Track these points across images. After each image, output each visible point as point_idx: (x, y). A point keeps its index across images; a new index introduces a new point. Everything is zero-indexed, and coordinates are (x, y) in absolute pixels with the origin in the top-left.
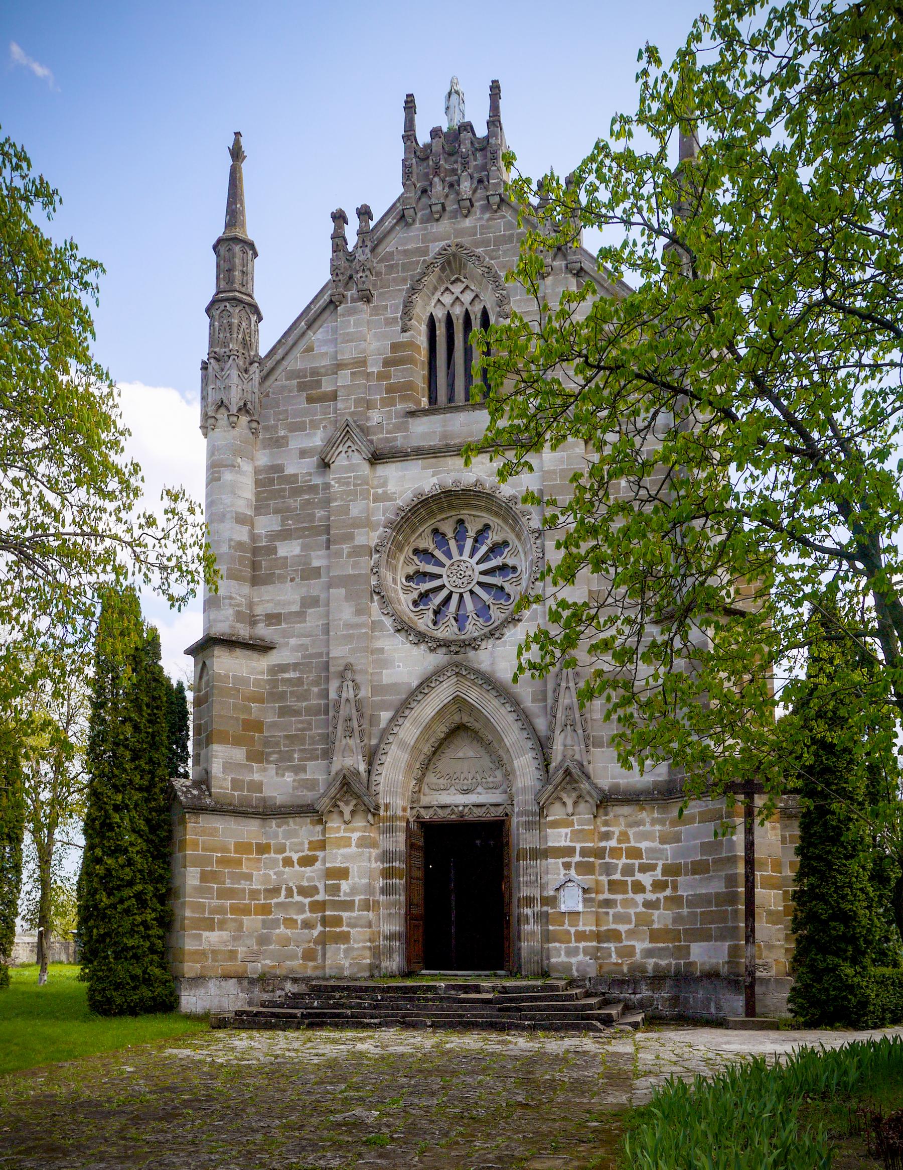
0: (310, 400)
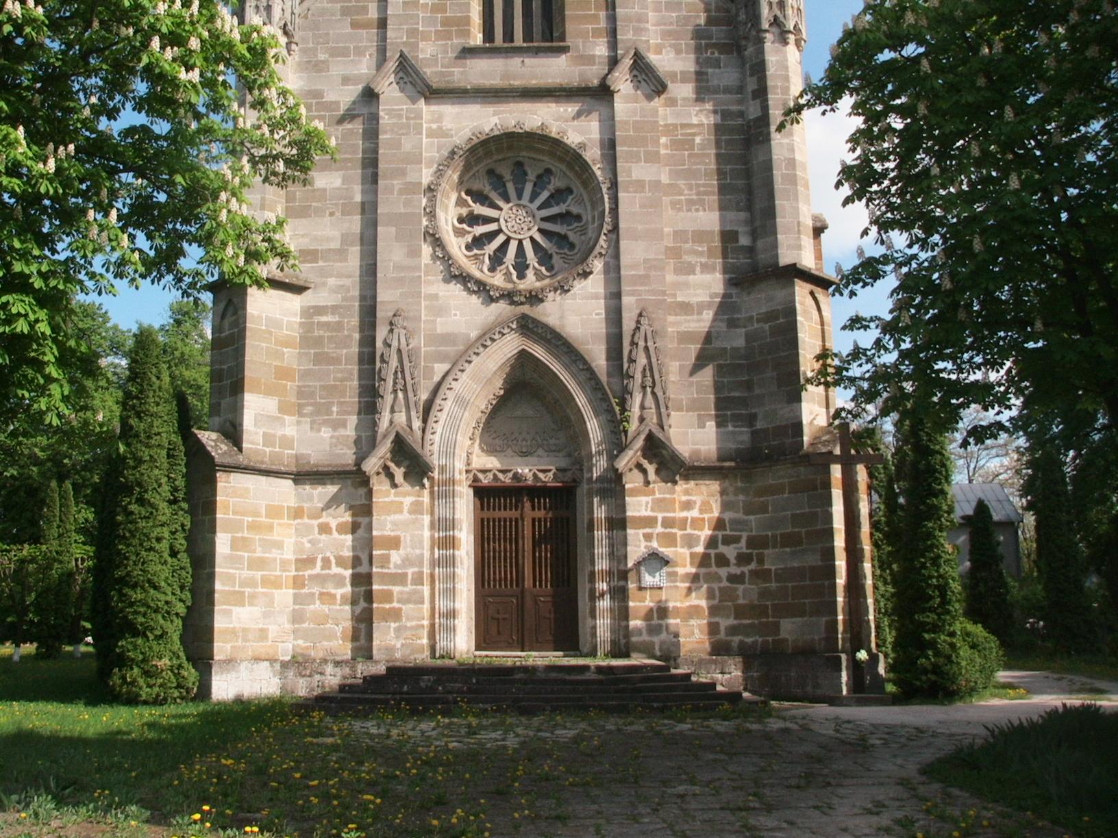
0: (355, 25)
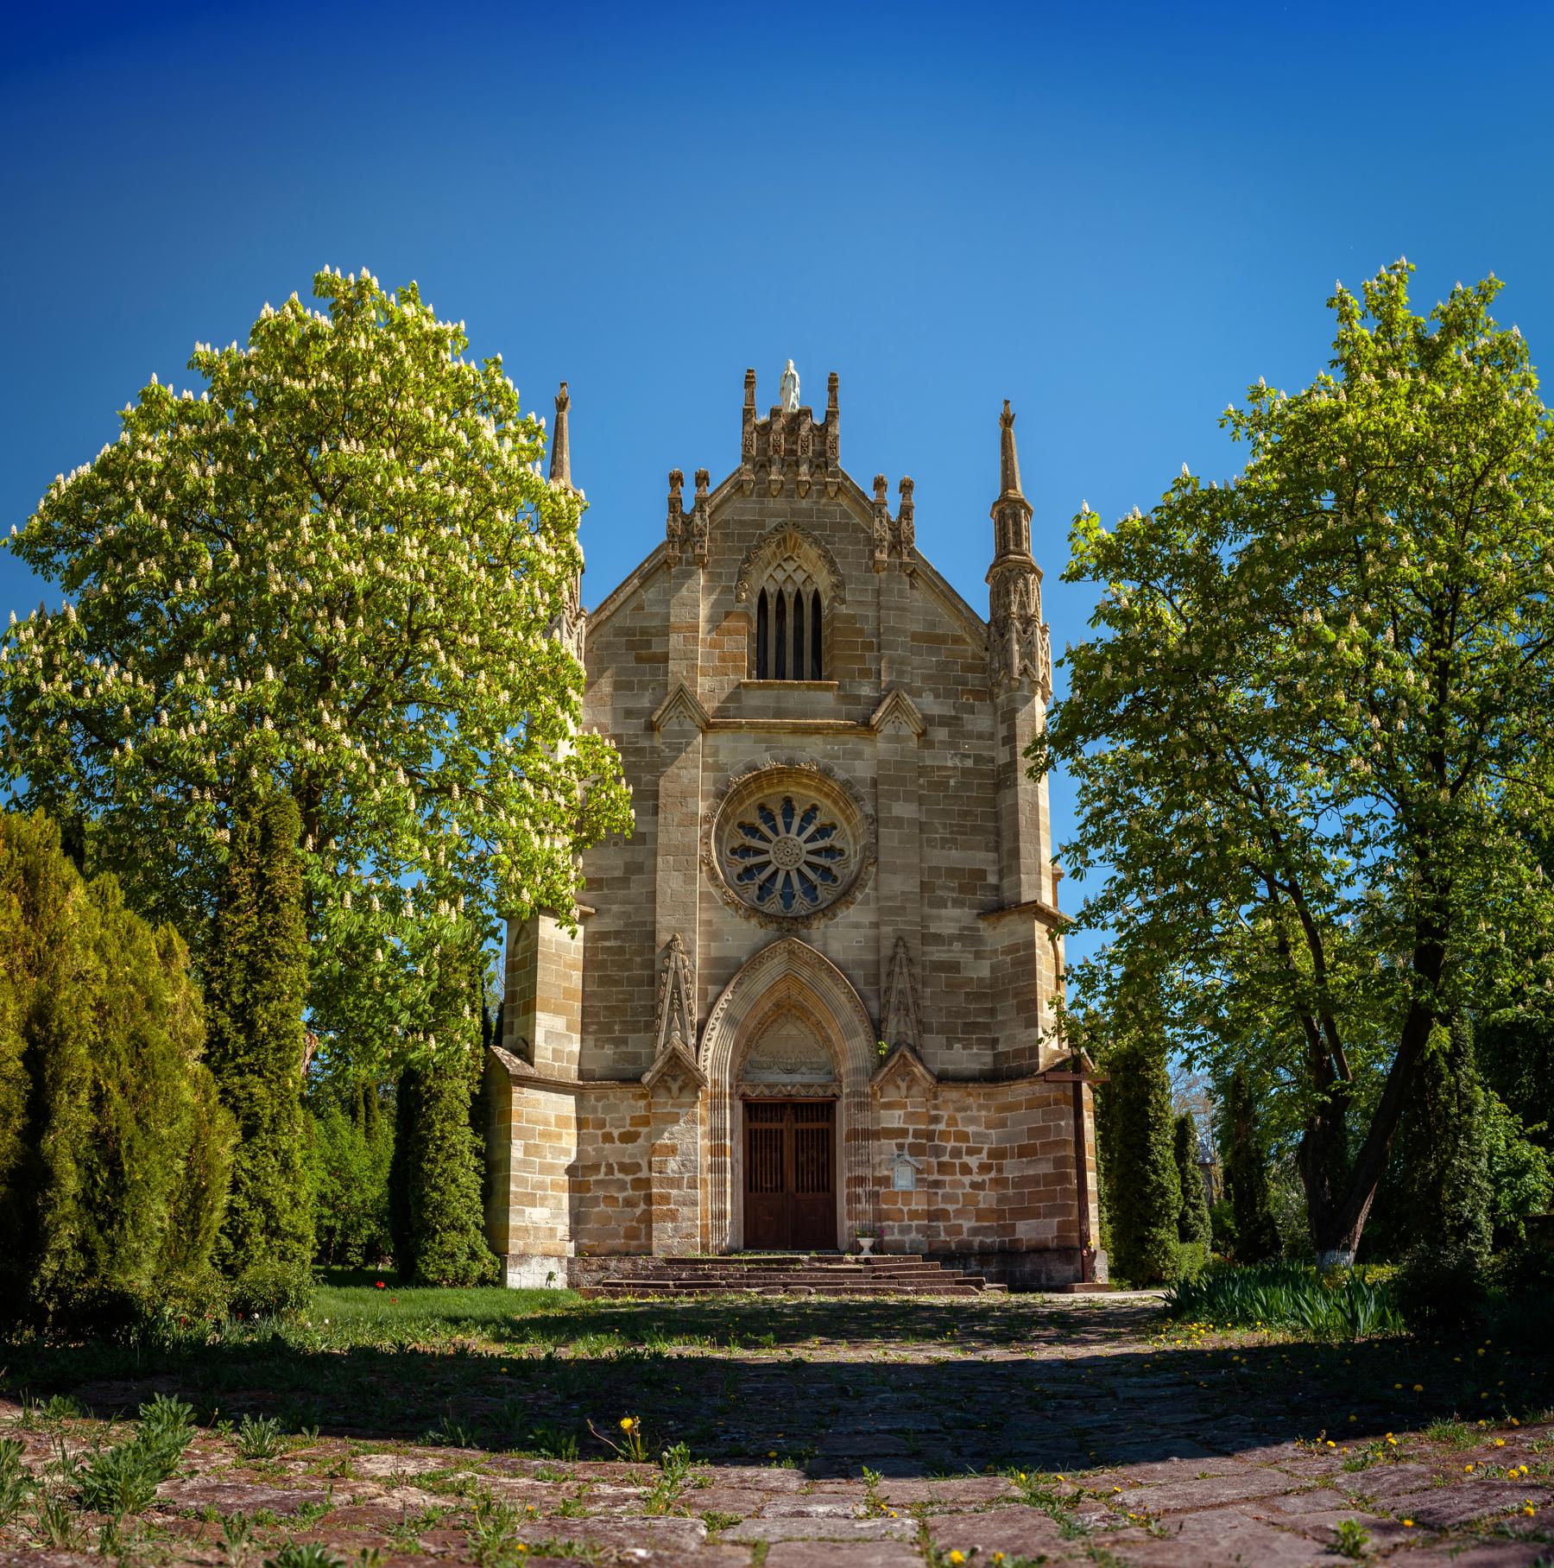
0: (639, 659)
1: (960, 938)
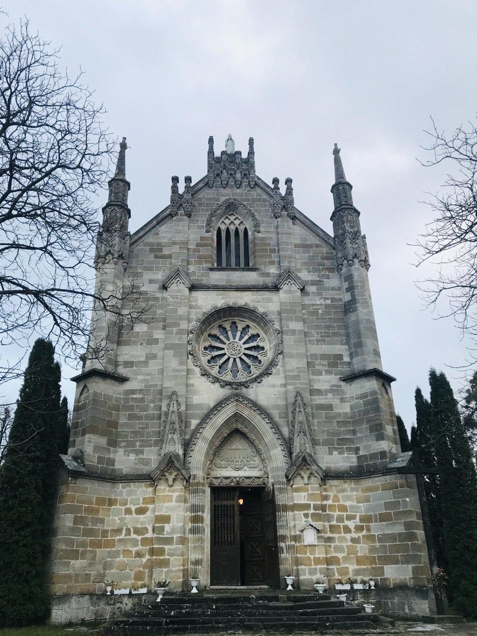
0: (156, 257)
1: (331, 391)
